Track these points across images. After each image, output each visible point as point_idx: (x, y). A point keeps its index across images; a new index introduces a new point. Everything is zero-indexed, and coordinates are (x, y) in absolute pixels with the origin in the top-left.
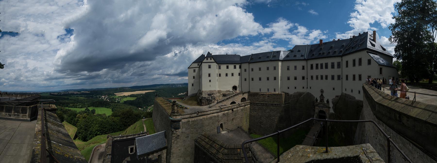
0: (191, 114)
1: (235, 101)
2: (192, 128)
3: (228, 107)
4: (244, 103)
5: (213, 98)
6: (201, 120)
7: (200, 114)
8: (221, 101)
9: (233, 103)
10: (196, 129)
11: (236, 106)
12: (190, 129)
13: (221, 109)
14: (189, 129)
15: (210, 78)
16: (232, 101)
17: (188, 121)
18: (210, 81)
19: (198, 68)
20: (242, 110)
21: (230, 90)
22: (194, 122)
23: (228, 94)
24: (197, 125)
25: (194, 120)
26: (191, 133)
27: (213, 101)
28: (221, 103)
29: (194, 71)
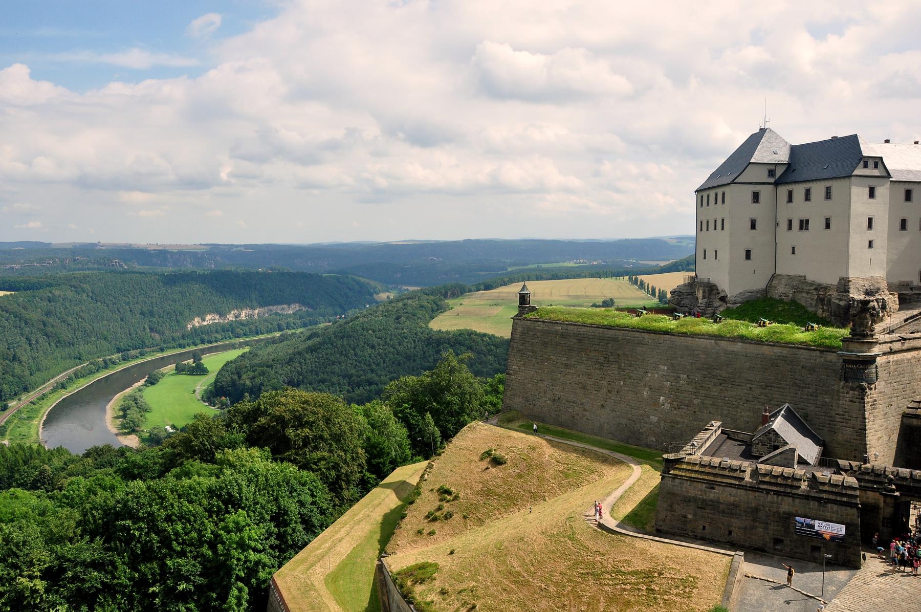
0: (891, 342)
2: (895, 381)
5: (880, 304)
6: (909, 360)
7: (907, 345)
14: (890, 383)
15: (871, 235)
17: (887, 361)
18: (870, 244)
19: (771, 186)
21: (912, 282)
22: (897, 364)
24: (903, 374)
25: (897, 361)
27: (881, 315)
29: (756, 197)
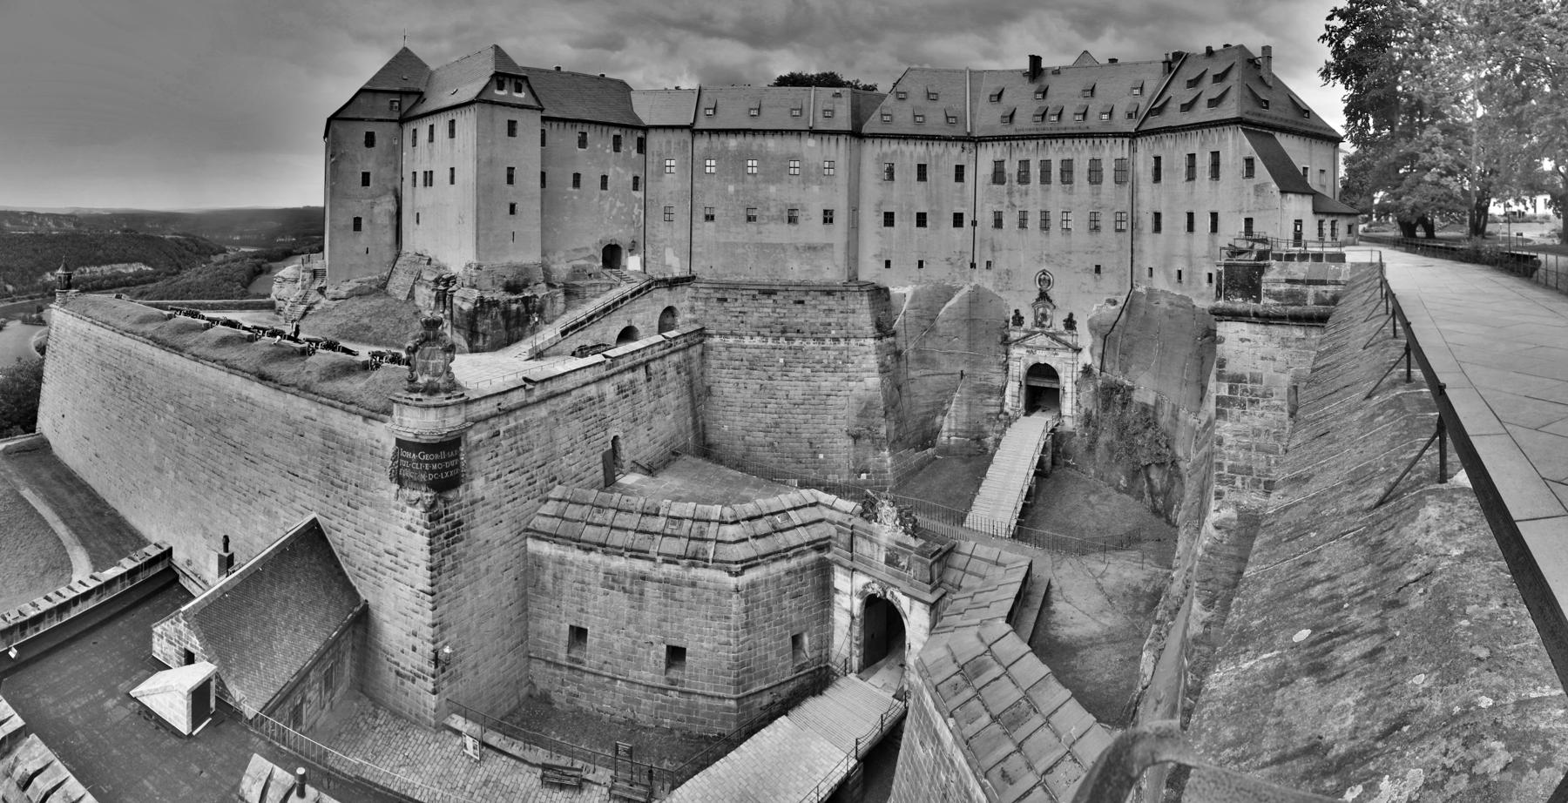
1: (637, 326)
2: (513, 468)
3: (632, 353)
4: (684, 335)
8: (582, 323)
9: (627, 334)
10: (528, 475)
11: (656, 348)
12: (503, 479)
13: (609, 360)
14: (499, 477)
16: (626, 324)
20: (678, 367)
23: (591, 285)
24: (525, 451)
26: (511, 498)
28: (580, 334)
